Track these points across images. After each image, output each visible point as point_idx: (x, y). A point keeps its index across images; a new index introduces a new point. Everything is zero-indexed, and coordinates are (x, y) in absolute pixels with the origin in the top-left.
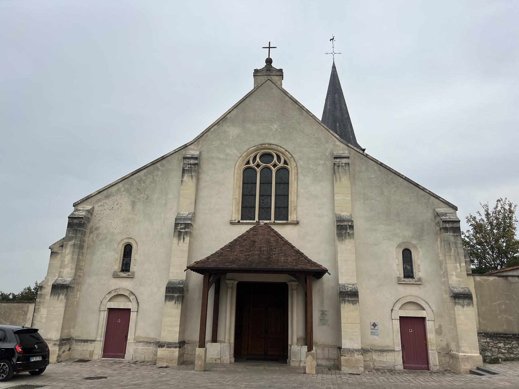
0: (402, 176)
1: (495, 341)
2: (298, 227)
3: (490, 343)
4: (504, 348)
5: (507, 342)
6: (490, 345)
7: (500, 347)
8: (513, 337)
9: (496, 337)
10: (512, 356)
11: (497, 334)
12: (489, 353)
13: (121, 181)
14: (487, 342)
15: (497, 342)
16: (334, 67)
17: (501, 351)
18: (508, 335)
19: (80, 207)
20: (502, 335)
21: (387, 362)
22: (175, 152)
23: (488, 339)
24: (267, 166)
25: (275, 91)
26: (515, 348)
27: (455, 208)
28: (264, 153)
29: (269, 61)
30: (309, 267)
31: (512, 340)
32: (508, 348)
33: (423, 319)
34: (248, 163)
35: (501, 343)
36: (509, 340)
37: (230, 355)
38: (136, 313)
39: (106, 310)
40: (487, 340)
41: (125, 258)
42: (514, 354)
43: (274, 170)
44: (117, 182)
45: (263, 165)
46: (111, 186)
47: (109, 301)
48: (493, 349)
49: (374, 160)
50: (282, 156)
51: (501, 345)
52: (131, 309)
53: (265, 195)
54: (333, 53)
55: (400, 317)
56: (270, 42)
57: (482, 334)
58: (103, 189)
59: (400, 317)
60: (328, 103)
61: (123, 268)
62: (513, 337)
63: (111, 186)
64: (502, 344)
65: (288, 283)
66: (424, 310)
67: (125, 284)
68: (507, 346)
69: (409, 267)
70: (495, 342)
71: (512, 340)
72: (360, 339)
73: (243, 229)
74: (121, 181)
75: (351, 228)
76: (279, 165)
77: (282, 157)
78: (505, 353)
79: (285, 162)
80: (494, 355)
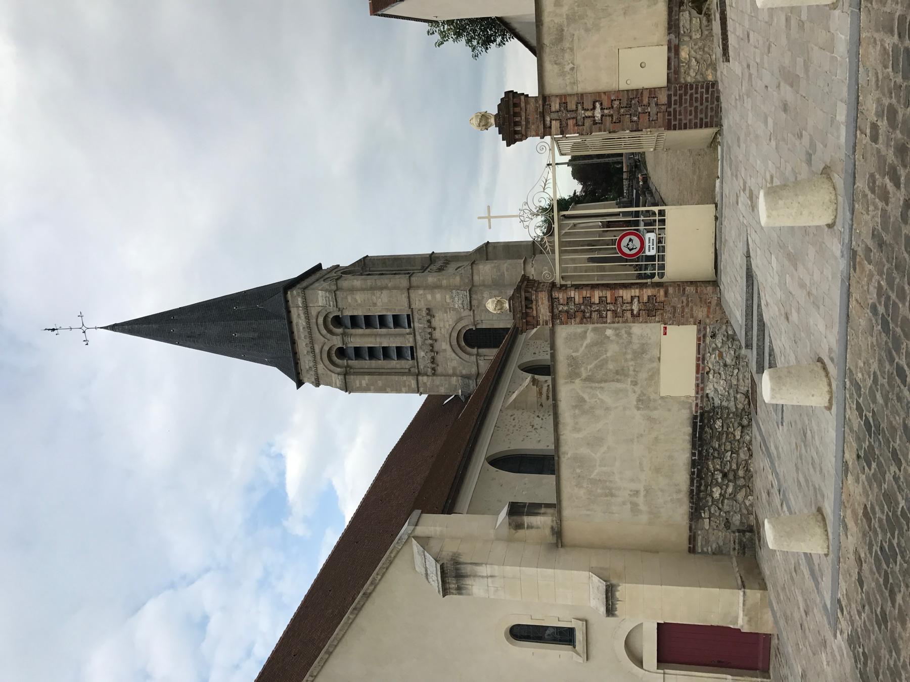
1: (707, 502)
3: (712, 512)
4: (724, 487)
5: (710, 479)
6: (717, 514)
7: (720, 494)
8: (699, 467)
9: (699, 499)
10: (741, 473)
12: (734, 518)
14: (709, 518)
15: (710, 499)
16: (114, 328)
17: (730, 495)
18: (695, 476)
20: (694, 488)
26: (725, 465)
31: (705, 469)
32: (722, 479)
33: (662, 628)
36: (706, 474)
42: (738, 469)
48: (726, 508)
62: (699, 467)
64: (714, 490)
68: (720, 480)
70: (710, 504)
71: (705, 469)
78: (734, 486)
80: (739, 509)
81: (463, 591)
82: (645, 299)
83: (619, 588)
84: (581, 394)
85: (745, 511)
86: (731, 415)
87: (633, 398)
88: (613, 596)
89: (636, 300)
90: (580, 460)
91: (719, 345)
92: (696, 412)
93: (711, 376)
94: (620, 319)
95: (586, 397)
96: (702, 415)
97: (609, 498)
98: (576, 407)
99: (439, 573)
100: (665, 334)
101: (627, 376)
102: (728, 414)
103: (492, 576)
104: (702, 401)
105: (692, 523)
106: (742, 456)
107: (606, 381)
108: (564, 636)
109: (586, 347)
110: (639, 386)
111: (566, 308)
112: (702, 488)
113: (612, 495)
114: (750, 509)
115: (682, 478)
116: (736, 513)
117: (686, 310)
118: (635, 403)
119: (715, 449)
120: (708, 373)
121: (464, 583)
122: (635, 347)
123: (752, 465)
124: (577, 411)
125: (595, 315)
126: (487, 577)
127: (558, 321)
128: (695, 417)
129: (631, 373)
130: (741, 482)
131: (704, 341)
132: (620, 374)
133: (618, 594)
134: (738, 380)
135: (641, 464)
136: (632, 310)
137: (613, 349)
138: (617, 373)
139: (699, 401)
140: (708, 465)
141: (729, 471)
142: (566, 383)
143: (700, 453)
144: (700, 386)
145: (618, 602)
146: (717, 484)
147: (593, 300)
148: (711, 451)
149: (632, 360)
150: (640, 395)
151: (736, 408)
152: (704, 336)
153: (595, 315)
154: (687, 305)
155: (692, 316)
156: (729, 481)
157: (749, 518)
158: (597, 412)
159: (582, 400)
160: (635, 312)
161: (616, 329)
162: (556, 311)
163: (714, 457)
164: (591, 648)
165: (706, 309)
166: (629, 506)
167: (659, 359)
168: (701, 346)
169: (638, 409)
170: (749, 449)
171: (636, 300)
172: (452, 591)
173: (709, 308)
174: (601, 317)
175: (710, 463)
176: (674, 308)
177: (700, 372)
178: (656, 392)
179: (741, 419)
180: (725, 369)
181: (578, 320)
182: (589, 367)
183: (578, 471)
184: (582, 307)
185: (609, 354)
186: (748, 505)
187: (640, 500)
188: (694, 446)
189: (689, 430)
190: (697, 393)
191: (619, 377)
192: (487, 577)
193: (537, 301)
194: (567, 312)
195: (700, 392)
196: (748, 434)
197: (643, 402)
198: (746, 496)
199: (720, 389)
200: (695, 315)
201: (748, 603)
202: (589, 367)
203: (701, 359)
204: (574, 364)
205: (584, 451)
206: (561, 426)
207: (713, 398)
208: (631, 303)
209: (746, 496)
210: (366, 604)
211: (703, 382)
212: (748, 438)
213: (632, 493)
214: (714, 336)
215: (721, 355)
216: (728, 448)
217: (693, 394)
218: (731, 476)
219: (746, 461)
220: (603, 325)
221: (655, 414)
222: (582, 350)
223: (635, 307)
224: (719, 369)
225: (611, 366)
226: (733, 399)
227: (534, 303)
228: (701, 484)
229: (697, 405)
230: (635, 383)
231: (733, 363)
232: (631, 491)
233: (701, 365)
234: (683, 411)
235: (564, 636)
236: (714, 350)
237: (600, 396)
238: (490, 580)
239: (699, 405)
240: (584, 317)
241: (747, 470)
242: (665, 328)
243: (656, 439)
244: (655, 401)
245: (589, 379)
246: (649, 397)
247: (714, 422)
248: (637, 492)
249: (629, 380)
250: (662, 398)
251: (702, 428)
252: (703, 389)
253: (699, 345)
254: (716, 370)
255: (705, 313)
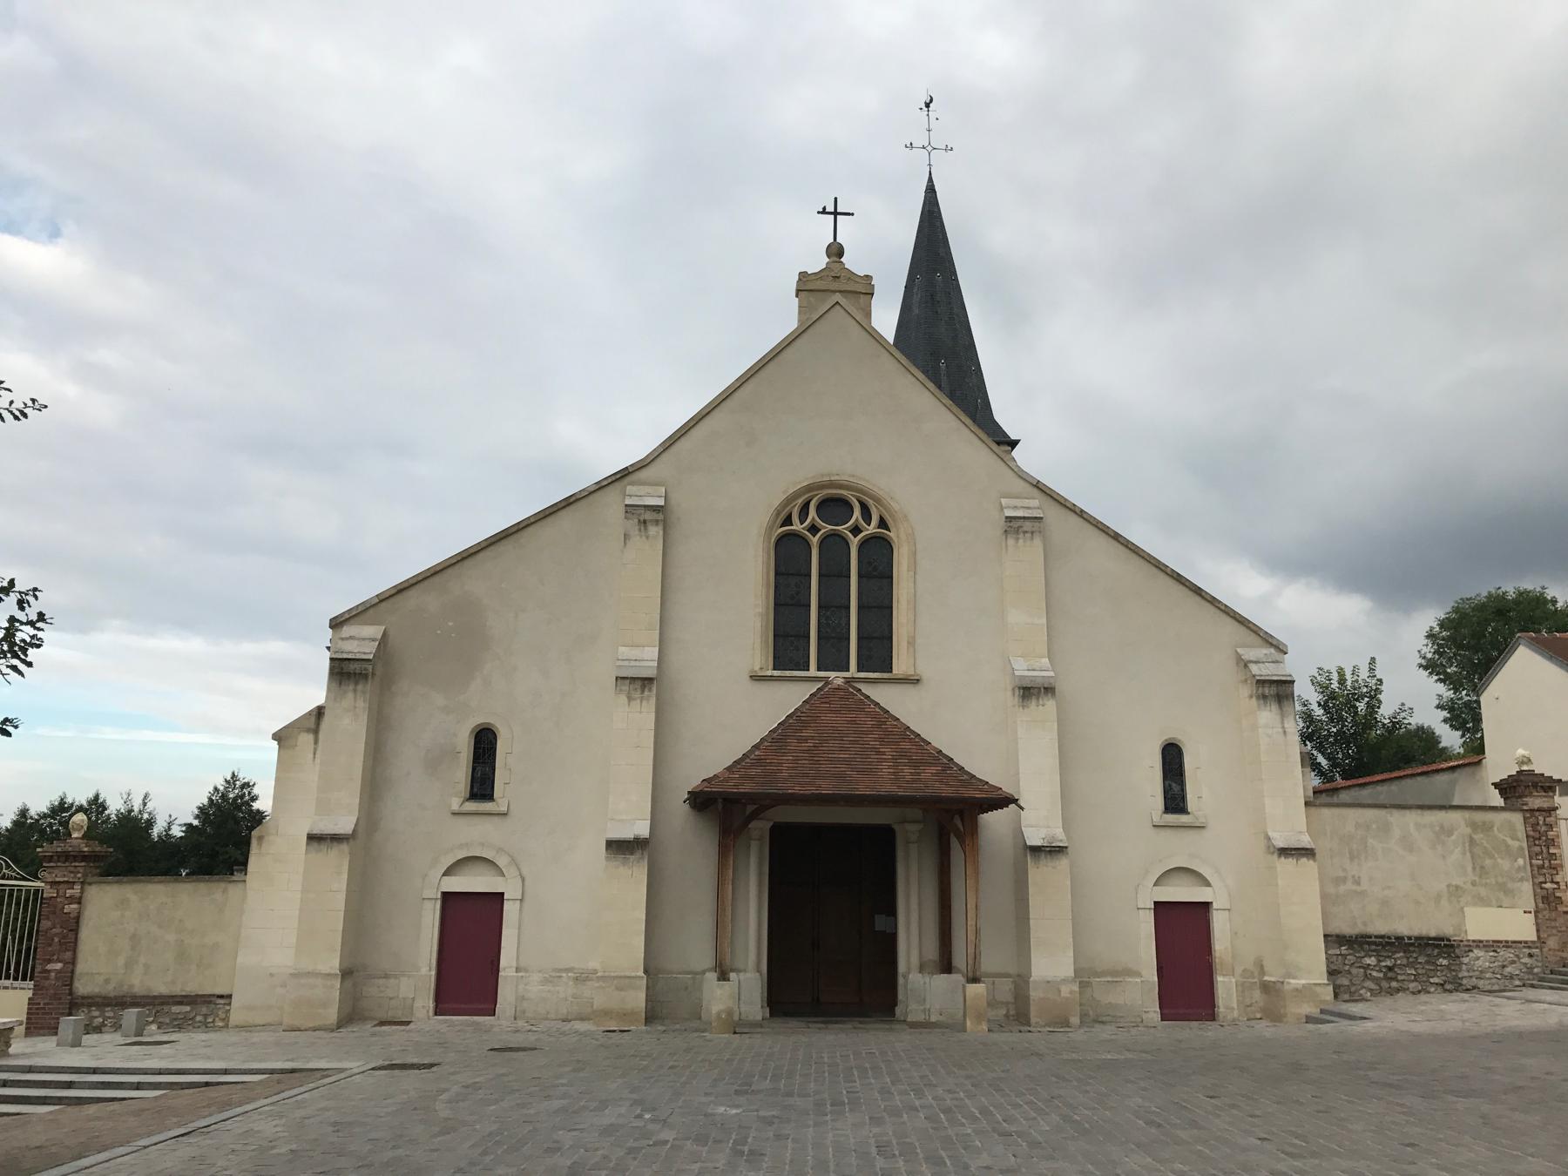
0: (1163, 568)
1: (1359, 952)
2: (918, 687)
3: (1348, 957)
4: (1377, 969)
5: (1385, 954)
6: (1347, 962)
7: (1369, 965)
9: (1361, 945)
10: (1394, 984)
11: (1362, 936)
12: (1344, 979)
13: (458, 562)
14: (1340, 955)
15: (1363, 954)
16: (931, 190)
19: (347, 631)
20: (1373, 939)
21: (1094, 1017)
22: (601, 486)
23: (1343, 948)
24: (836, 532)
25: (856, 331)
26: (1400, 969)
27: (1281, 649)
28: (829, 496)
29: (836, 251)
30: (994, 795)
32: (1386, 966)
33: (1206, 906)
34: (788, 521)
35: (1370, 956)
37: (762, 1001)
38: (519, 902)
39: (439, 896)
40: (1340, 950)
41: (479, 763)
42: (1398, 981)
43: (854, 542)
44: (447, 564)
45: (826, 528)
46: (432, 575)
47: (444, 875)
48: (1354, 971)
49: (1099, 525)
50: (876, 507)
51: (1371, 961)
52: (502, 894)
53: (834, 607)
54: (929, 148)
55: (1155, 903)
56: (836, 199)
57: (1333, 940)
58: (411, 582)
59: (1155, 903)
60: (916, 299)
61: (475, 790)
63: (432, 575)
64: (1373, 958)
65: (895, 827)
66: (1208, 884)
67: (477, 834)
68: (1384, 964)
69: (1176, 787)
70: (1357, 955)
72: (1072, 954)
73: (790, 696)
74: (458, 562)
75: (1050, 695)
76: (868, 530)
77: (873, 507)
79: (883, 523)
81: (1262, 702)
82: (1557, 894)
83: (1311, 862)
84: (1456, 833)
85: (1353, 989)
86: (1454, 974)
87: (1457, 881)
88: (1303, 855)
89: (1555, 886)
90: (1386, 829)
91: (1522, 960)
92: (1454, 941)
93: (1492, 954)
94: (1536, 872)
95: (1453, 837)
96: (1452, 946)
97: (1348, 855)
98: (1442, 827)
99: (1284, 678)
100: (1525, 912)
101: (1480, 877)
102: (1454, 970)
103: (1285, 732)
104: (1466, 946)
105: (1334, 938)
106: (1412, 986)
107: (1472, 857)
108: (1175, 801)
109: (1504, 840)
110: (1471, 887)
111: (1541, 822)
112: (1373, 947)
113: (1352, 858)
114: (1357, 994)
115: (1380, 927)
116: (1351, 980)
117: (1554, 931)
118: (1454, 883)
119: (1416, 958)
120: (1494, 951)
121: (1273, 707)
122: (1510, 885)
123: (1404, 995)
124: (1437, 828)
125: (1537, 849)
126: (1283, 727)
127: (1528, 815)
128: (1449, 940)
129: (1484, 881)
130: (1385, 984)
131: (1524, 947)
132: (1482, 871)
133: (1304, 860)
134: (1491, 979)
135: (1389, 888)
136: (1545, 883)
137: (1505, 864)
138: (1482, 867)
139: (1466, 943)
140: (1399, 952)
141: (1395, 972)
142: (1466, 820)
143: (1412, 945)
144: (1479, 944)
145: (1295, 860)
146: (1380, 961)
147: (1552, 847)
148: (1415, 955)
149: (1497, 883)
150: (1462, 888)
151: (1462, 978)
152: (1529, 947)
153: (1537, 849)
154: (1559, 931)
155: (1549, 936)
156: (1385, 974)
157: (1346, 993)
158: (1439, 848)
159: (1450, 833)
160: (1543, 885)
161: (1525, 867)
162: (1537, 814)
163: (1408, 958)
164: (1169, 832)
165: (1557, 948)
166: (1342, 874)
167: (1501, 907)
168: (1519, 945)
169: (1448, 886)
170: (1419, 992)
171: (1555, 886)
172: (1260, 689)
173: (1559, 950)
174: (1537, 854)
175: (1401, 954)
176: (1555, 920)
177: (1495, 944)
178: (1467, 904)
179: (1450, 983)
180: (1499, 966)
181: (1531, 833)
182: (1484, 842)
183: (1374, 826)
184: (1544, 838)
185: (1499, 860)
186: (1361, 992)
187: (1350, 886)
188: (1417, 938)
189: (1433, 934)
190: (1474, 941)
191: (1478, 869)
192: (1283, 727)
193: (1545, 796)
194: (1538, 824)
195: (1475, 944)
196: (1436, 990)
197: (1455, 891)
198: (1371, 990)
199: (1479, 963)
200: (1551, 938)
201: (1313, 987)
202: (1484, 842)
203: (1508, 945)
204: (1487, 828)
205: (1397, 832)
206: (1419, 812)
207: (1468, 956)
208: (1552, 882)
209: (1371, 990)
210: (1187, 590)
211: (1484, 946)
212: (1432, 990)
213: (1356, 878)
214: (1530, 955)
215: (1513, 962)
216: (1420, 972)
217: (1470, 938)
218: (1390, 975)
219: (1408, 989)
220: (1527, 856)
221: (1444, 902)
222: (1501, 836)
223: (1548, 885)
224: (1499, 961)
225: (1488, 862)
226: (1471, 974)
227: (1544, 794)
228: (1377, 945)
229: (1462, 941)
230: (1474, 884)
231: (1506, 974)
232: (1359, 877)
233: (1501, 945)
234: (1452, 928)
235: (1175, 801)
236: (1517, 956)
237: (1456, 851)
238: (1281, 730)
239: (1461, 944)
240: (1535, 839)
241: (1398, 990)
242: (1530, 912)
243: (1418, 903)
244: (1459, 902)
245: (1472, 841)
246: (1460, 897)
247: (1444, 958)
248: (1358, 883)
249: (1477, 879)
250: (1462, 908)
251: (1438, 946)
252: (1478, 946)
253: (1520, 942)
254: (1499, 958)
255: (1552, 947)
